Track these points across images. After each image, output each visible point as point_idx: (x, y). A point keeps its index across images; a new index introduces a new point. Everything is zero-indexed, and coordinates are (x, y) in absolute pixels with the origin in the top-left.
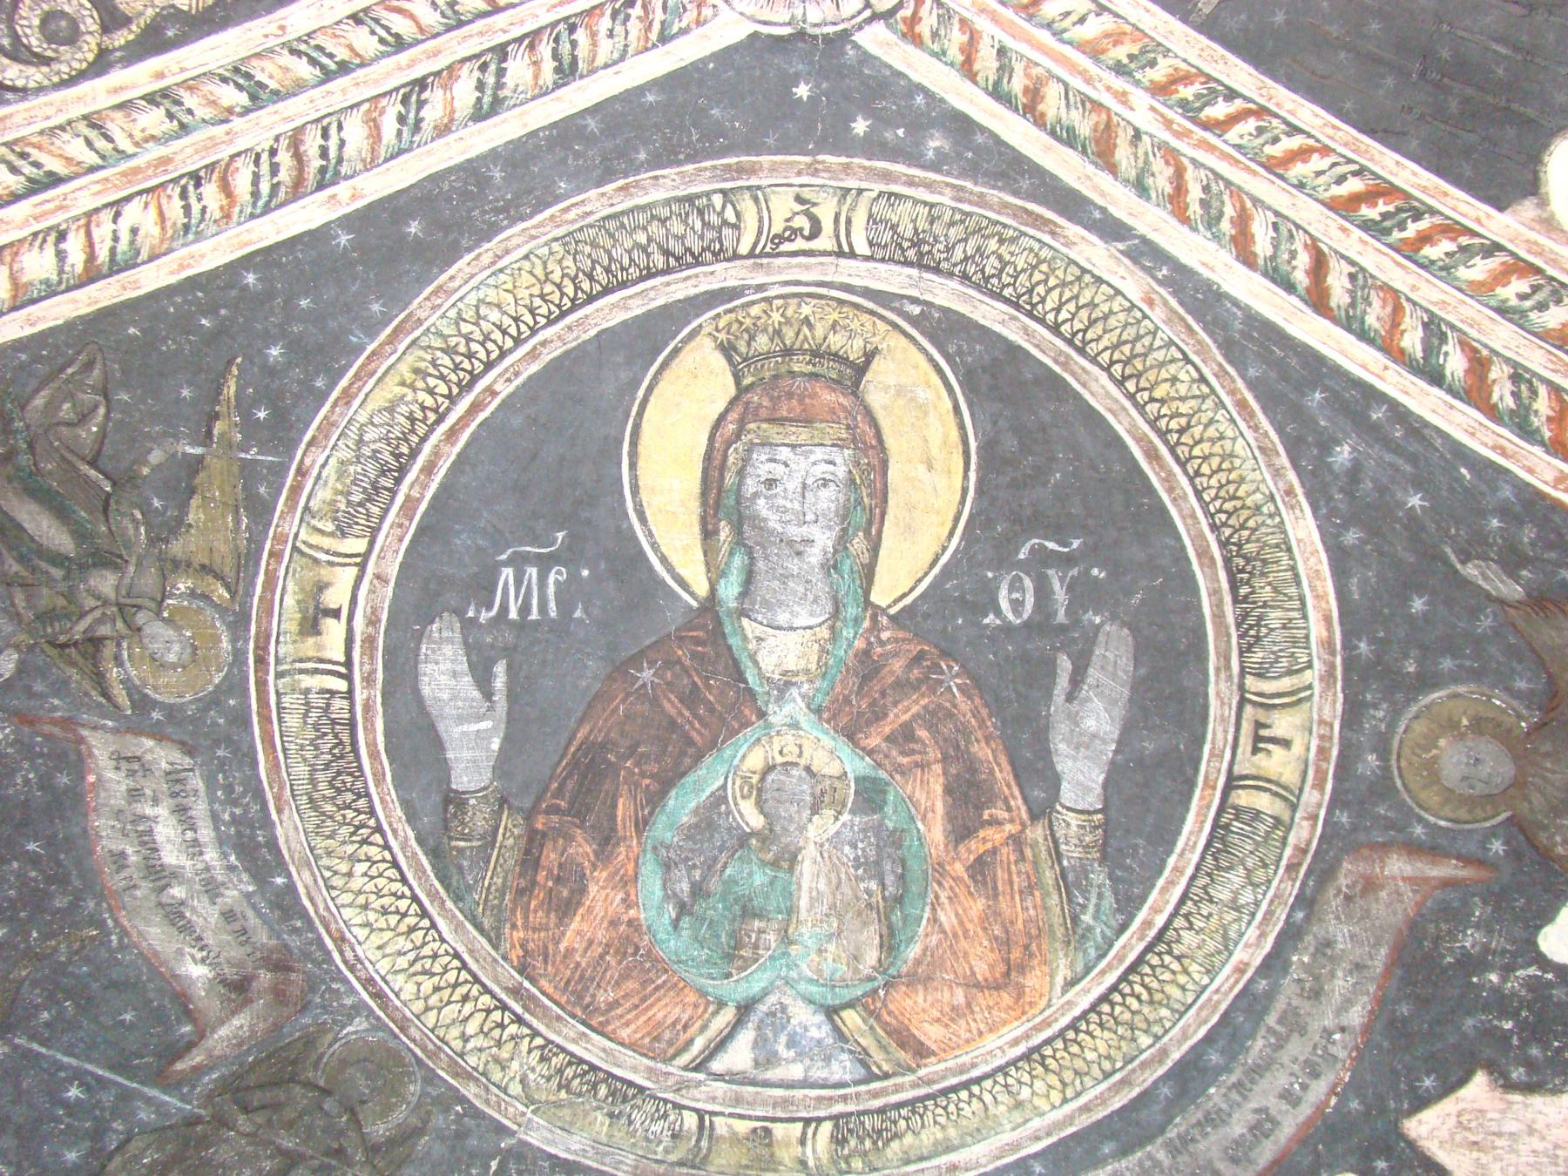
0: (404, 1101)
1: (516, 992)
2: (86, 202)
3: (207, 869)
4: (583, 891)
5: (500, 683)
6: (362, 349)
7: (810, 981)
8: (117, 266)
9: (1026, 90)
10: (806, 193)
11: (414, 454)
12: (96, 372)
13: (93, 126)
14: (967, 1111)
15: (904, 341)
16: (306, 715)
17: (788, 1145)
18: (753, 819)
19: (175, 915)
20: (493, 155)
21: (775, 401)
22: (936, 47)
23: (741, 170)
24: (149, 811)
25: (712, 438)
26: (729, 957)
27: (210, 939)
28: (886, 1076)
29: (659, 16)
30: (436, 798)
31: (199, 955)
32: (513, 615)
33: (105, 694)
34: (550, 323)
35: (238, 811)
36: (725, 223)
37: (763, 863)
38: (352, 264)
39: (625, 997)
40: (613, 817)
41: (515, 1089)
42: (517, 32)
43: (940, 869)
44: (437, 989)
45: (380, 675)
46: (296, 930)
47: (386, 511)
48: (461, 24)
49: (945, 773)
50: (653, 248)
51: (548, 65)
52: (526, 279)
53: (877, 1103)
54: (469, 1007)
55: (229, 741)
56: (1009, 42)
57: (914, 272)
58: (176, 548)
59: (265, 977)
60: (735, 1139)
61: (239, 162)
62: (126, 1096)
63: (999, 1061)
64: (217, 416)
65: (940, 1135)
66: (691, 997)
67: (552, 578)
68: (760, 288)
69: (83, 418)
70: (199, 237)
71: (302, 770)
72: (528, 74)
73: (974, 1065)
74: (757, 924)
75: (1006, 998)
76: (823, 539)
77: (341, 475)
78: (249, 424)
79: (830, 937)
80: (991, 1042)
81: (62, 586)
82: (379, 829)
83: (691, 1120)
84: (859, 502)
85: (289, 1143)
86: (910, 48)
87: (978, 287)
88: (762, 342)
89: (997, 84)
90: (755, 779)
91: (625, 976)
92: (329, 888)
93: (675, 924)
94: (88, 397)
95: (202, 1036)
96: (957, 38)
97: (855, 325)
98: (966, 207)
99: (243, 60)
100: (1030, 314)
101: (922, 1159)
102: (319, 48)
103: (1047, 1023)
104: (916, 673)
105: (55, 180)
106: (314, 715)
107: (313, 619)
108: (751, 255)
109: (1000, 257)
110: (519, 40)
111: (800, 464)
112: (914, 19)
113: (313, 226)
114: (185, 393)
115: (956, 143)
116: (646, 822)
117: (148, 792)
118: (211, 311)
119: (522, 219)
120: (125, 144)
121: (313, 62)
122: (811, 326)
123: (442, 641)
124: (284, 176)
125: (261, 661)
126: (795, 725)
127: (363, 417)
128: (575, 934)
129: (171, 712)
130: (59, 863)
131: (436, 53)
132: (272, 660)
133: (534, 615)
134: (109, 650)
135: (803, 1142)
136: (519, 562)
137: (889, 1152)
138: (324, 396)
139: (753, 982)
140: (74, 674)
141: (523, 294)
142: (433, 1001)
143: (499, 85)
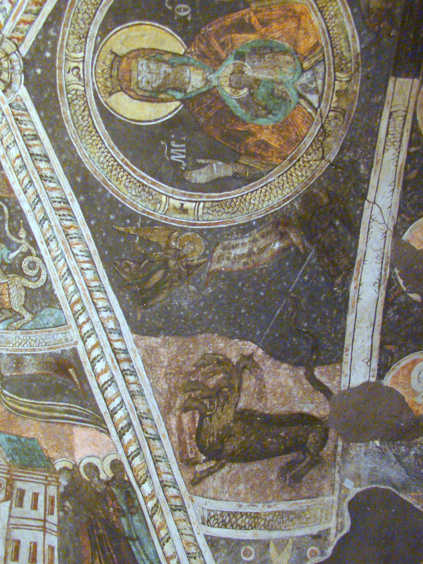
0: (318, 194)
1: (291, 161)
2: (74, 263)
3: (249, 241)
4: (263, 141)
5: (203, 161)
6: (111, 194)
7: (294, 77)
8: (90, 255)
9: (36, 5)
10: (67, 70)
11: (139, 182)
12: (117, 262)
13: (55, 259)
14: (336, 31)
15: (108, 43)
17: (341, 86)
18: (244, 92)
19: (261, 251)
20: (59, 157)
21: (125, 80)
22: (25, 32)
23: (61, 89)
24: (233, 256)
25: (136, 99)
26: (285, 100)
27: (268, 242)
28: (324, 55)
29: (20, 112)
30: (234, 180)
32: (184, 157)
33: (201, 264)
34: (104, 143)
36: (76, 94)
37: (258, 89)
38: (88, 196)
39: (294, 130)
40: (242, 132)
41: (318, 163)
42: (26, 150)
43: (263, 36)
44: (288, 183)
45: (200, 194)
46: (269, 219)
47: (155, 190)
48: (25, 165)
49: (234, 33)
50: (83, 114)
51: (35, 142)
52: (92, 150)
53: (331, 58)
54: (294, 174)
56: (23, 10)
57: (88, 40)
58: (163, 245)
59: (280, 228)
60: (338, 101)
61: (63, 224)
62: (309, 265)
63: (322, 21)
64: (129, 233)
65: (343, 40)
66: (296, 112)
67: (174, 145)
68: (93, 84)
69: (129, 266)
70: (82, 235)
71: (224, 216)
72: (37, 148)
73: (323, 29)
74: (276, 91)
75: (303, 17)
76: (165, 68)
77: (145, 201)
78: (131, 225)
79: (281, 70)
80: (316, 22)
82: (242, 196)
83: (332, 114)
84: (154, 57)
85: (327, 224)
86: (26, 40)
87: (92, 20)
88: (108, 84)
89: (35, 14)
90: (233, 90)
91: (288, 130)
92: (257, 210)
93: (274, 115)
94: (123, 264)
95: (295, 245)
96: (22, 26)
97: (103, 57)
98: (70, 24)
99: (37, 221)
100: (100, 5)
101: (349, 46)
102: (33, 202)
103: (312, 5)
104: (204, 41)
105: (68, 269)
106: (209, 211)
107: (183, 211)
108: (84, 86)
109: (84, 13)
110: (28, 150)
111: (144, 74)
112: (18, 39)
113: (79, 206)
115: (51, 26)
116: (244, 122)
118: (101, 233)
119: (75, 150)
120: (59, 252)
121: (37, 204)
122: (104, 70)
123: (191, 177)
124: (65, 213)
125: (194, 225)
126: (218, 78)
127: (130, 195)
128: (274, 143)
129: (207, 248)
131: (33, 172)
133: (184, 151)
134: (189, 263)
135: (341, 81)
136: (170, 155)
137: (347, 56)
138: (124, 205)
139: (292, 94)
140: (195, 272)
141: (96, 151)
142: (291, 184)
143: (40, 155)
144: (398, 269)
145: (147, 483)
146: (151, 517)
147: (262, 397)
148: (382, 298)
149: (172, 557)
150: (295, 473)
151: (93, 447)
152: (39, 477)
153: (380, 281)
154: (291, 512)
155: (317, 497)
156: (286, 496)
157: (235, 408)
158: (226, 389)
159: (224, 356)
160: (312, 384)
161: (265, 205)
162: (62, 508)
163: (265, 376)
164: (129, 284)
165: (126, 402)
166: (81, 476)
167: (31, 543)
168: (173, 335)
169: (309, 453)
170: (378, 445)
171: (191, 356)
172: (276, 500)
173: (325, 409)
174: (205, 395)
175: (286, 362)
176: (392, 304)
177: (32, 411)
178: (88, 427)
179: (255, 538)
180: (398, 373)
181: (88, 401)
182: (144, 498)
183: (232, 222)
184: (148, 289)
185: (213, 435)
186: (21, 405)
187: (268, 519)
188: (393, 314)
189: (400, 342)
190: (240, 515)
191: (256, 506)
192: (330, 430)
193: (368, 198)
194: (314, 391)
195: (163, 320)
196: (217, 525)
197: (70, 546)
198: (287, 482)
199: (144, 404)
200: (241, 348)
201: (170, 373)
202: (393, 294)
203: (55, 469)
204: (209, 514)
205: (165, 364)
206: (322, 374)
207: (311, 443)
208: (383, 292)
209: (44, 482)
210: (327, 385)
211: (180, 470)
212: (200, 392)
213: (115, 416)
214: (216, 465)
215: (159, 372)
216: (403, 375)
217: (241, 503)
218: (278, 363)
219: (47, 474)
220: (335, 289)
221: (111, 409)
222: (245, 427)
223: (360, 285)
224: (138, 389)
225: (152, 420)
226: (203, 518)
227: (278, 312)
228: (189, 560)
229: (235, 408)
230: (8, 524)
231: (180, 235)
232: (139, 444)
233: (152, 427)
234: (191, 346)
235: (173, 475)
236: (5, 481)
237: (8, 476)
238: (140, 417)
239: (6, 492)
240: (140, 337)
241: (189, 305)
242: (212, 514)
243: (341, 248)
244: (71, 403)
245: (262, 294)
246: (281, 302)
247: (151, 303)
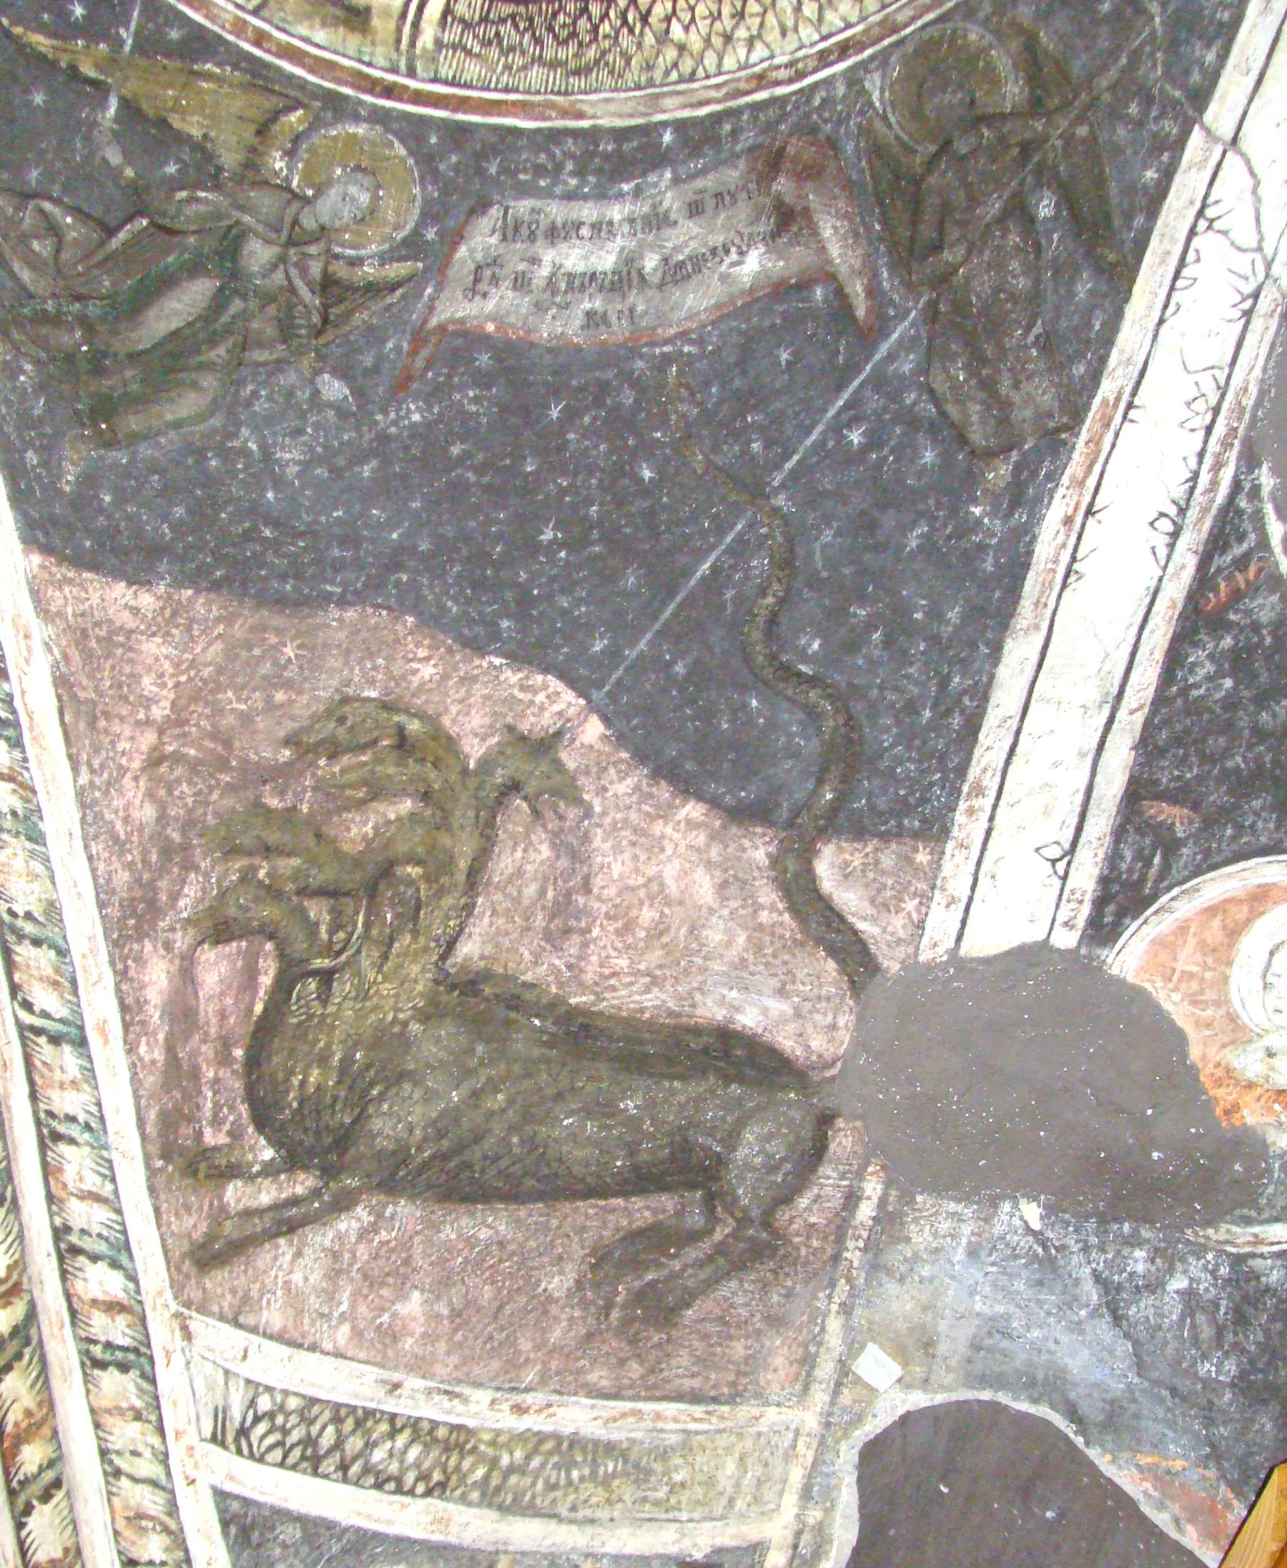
0: (985, 51)
3: (631, 221)
16: (469, 53)
24: (545, 271)
27: (719, 239)
31: (734, 256)
33: (393, 288)
35: (570, 166)
46: (734, 133)
55: (482, 156)
59: (782, 185)
62: (879, 382)
64: (73, 68)
69: (54, 230)
71: (536, 75)
81: (253, 304)
85: (995, 206)
92: (692, 77)
94: (28, 219)
106: (470, 42)
114: (39, 99)
117: (521, 267)
125: (389, 91)
129: (429, 216)
130: (582, 389)
132: (390, 78)
134: (340, 270)
140: (360, 317)
144: (1275, 471)
147: (567, 931)
148: (1176, 590)
150: (652, 1285)
153: (1182, 511)
154: (610, 1448)
155: (732, 1400)
156: (600, 1377)
157: (443, 958)
158: (413, 871)
159: (432, 721)
160: (794, 910)
161: (729, 63)
163: (597, 842)
164: (43, 318)
168: (216, 586)
169: (732, 1203)
170: (1036, 1225)
171: (280, 697)
172: (554, 1383)
173: (833, 1027)
174: (318, 878)
175: (700, 798)
176: (1218, 624)
179: (437, 1537)
180: (1183, 929)
183: (565, 114)
184: (131, 356)
185: (323, 1060)
187: (505, 1460)
188: (1209, 668)
189: (1217, 797)
190: (384, 1427)
191: (466, 1400)
192: (840, 1123)
193: (1208, 117)
194: (802, 944)
195: (179, 511)
196: (277, 1455)
198: (615, 1314)
200: (511, 701)
201: (177, 758)
202: (1229, 578)
204: (252, 1403)
205: (158, 713)
206: (846, 875)
207: (748, 1167)
208: (1186, 561)
210: (861, 925)
211: (152, 1190)
212: (296, 862)
214: (316, 1193)
215: (123, 745)
216: (1202, 944)
217: (396, 1376)
218: (664, 792)
220: (977, 511)
222: (471, 1051)
223: (1089, 512)
224: (19, 806)
225: (63, 953)
226: (220, 1415)
227: (706, 566)
229: (443, 958)
231: (312, 127)
233: (56, 984)
234: (289, 651)
235: (119, 1211)
240: (61, 572)
241: (306, 466)
242: (264, 1403)
243: (1038, 329)
245: (647, 474)
246: (721, 529)
247: (134, 423)
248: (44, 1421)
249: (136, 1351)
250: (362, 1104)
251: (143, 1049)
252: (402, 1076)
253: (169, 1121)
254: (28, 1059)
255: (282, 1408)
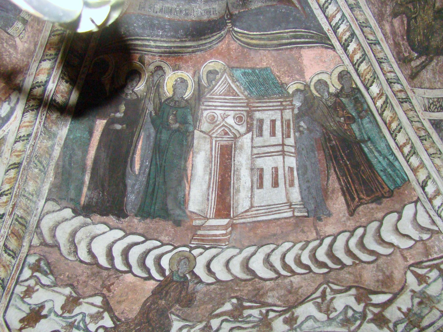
145: (374, 85)
146: (381, 115)
149: (405, 145)
151: (321, 64)
152: (275, 104)
157: (434, 8)
162: (298, 129)
165: (347, 15)
166: (312, 94)
167: (272, 168)
177: (262, 42)
178: (314, 47)
181: (311, 23)
182: (373, 99)
185: (419, 34)
186: (252, 39)
196: (436, 110)
197: (308, 163)
199: (361, 15)
203: (288, 93)
204: (429, 102)
209: (279, 108)
211: (399, 67)
213: (338, 30)
214: (426, 59)
219: (281, 100)
221: (334, 25)
225: (371, 28)
226: (424, 105)
228: (422, 142)
230: (252, 155)
232: (364, 50)
233: (371, 34)
235: (395, 73)
236: (245, 113)
237: (248, 109)
238: (361, 27)
239: (247, 125)
242: (431, 101)
244: (296, 28)
248: (395, 117)
249: (407, 98)
250: (428, 40)
251: (389, 42)
252: (433, 33)
253: (399, 53)
254: (371, 49)
255: (434, 101)
